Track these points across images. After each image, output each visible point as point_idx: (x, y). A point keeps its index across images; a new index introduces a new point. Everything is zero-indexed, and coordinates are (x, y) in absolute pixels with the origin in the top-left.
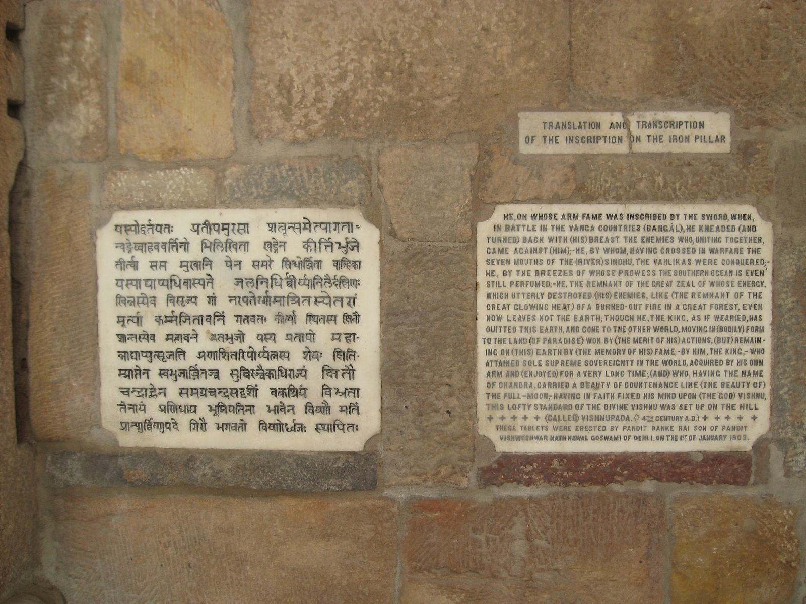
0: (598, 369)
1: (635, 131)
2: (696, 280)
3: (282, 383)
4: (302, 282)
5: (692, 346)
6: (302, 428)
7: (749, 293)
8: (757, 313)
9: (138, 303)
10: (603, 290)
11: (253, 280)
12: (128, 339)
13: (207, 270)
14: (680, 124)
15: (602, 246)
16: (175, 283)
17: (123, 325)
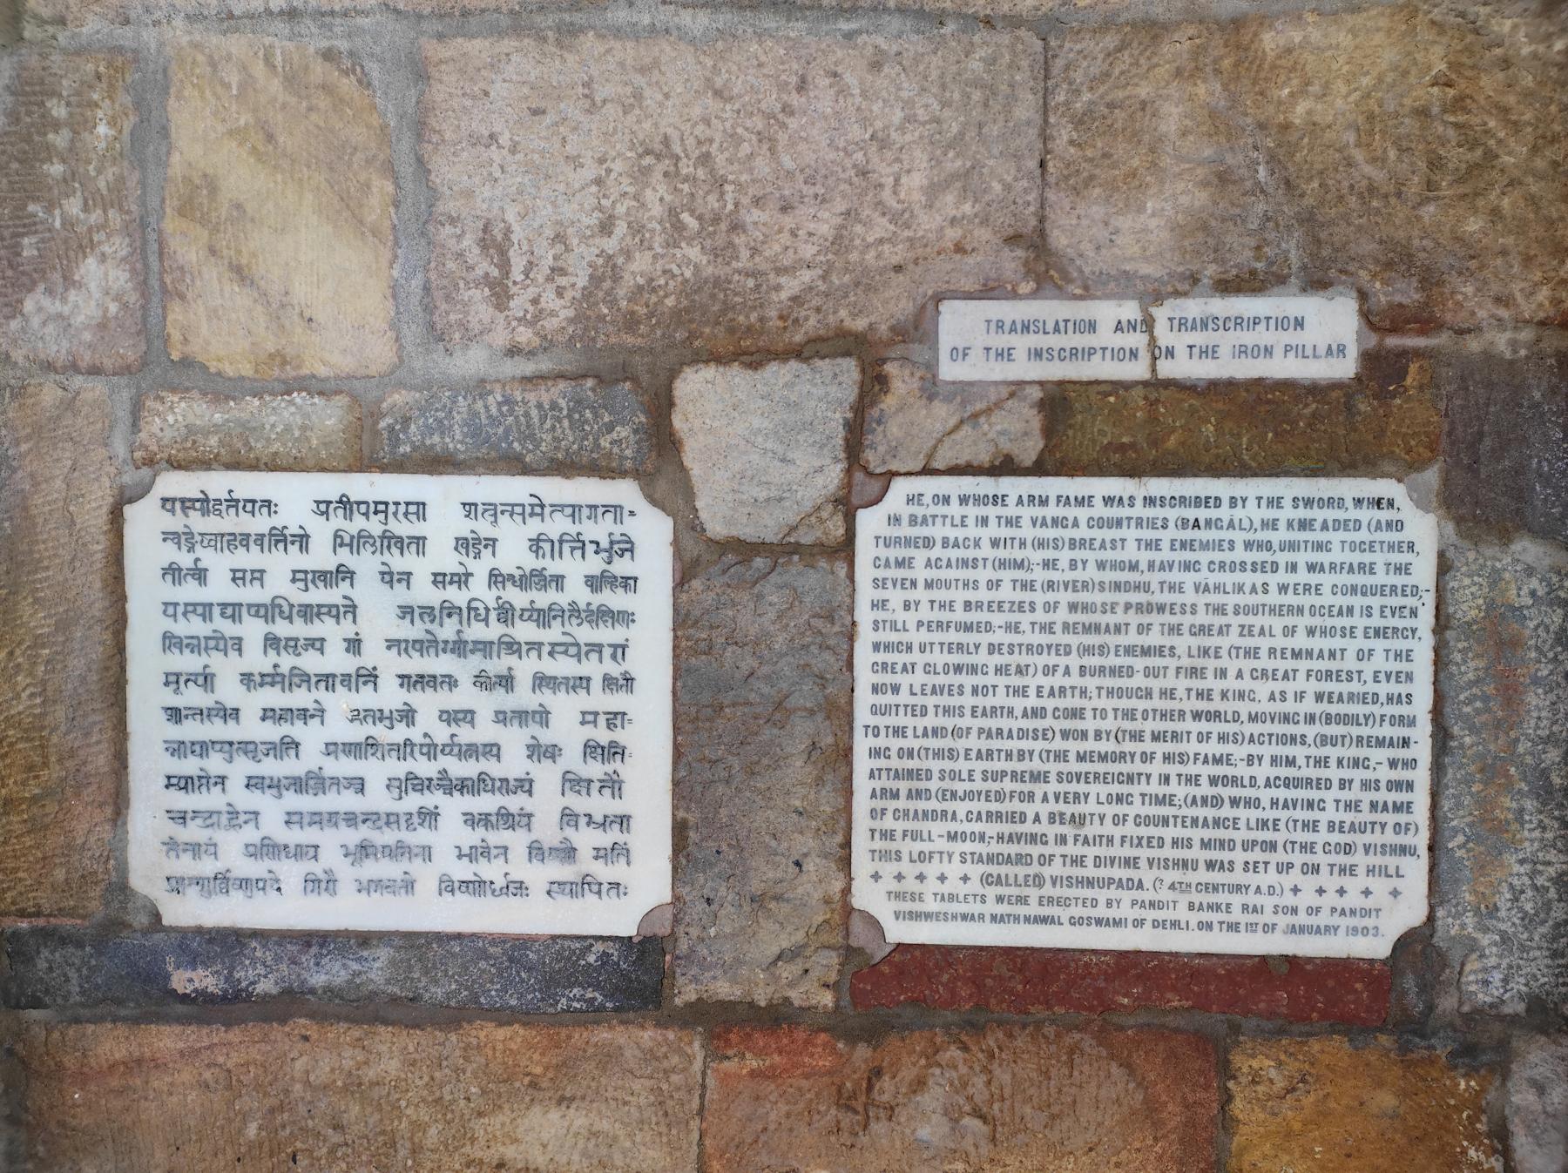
0: (1082, 788)
1: (1165, 337)
2: (1277, 623)
3: (487, 803)
4: (526, 615)
5: (1267, 751)
6: (518, 888)
7: (1387, 651)
8: (1403, 689)
9: (206, 649)
10: (1092, 639)
11: (432, 608)
12: (186, 717)
13: (345, 587)
14: (1256, 321)
15: (1091, 556)
16: (281, 612)
17: (177, 691)
